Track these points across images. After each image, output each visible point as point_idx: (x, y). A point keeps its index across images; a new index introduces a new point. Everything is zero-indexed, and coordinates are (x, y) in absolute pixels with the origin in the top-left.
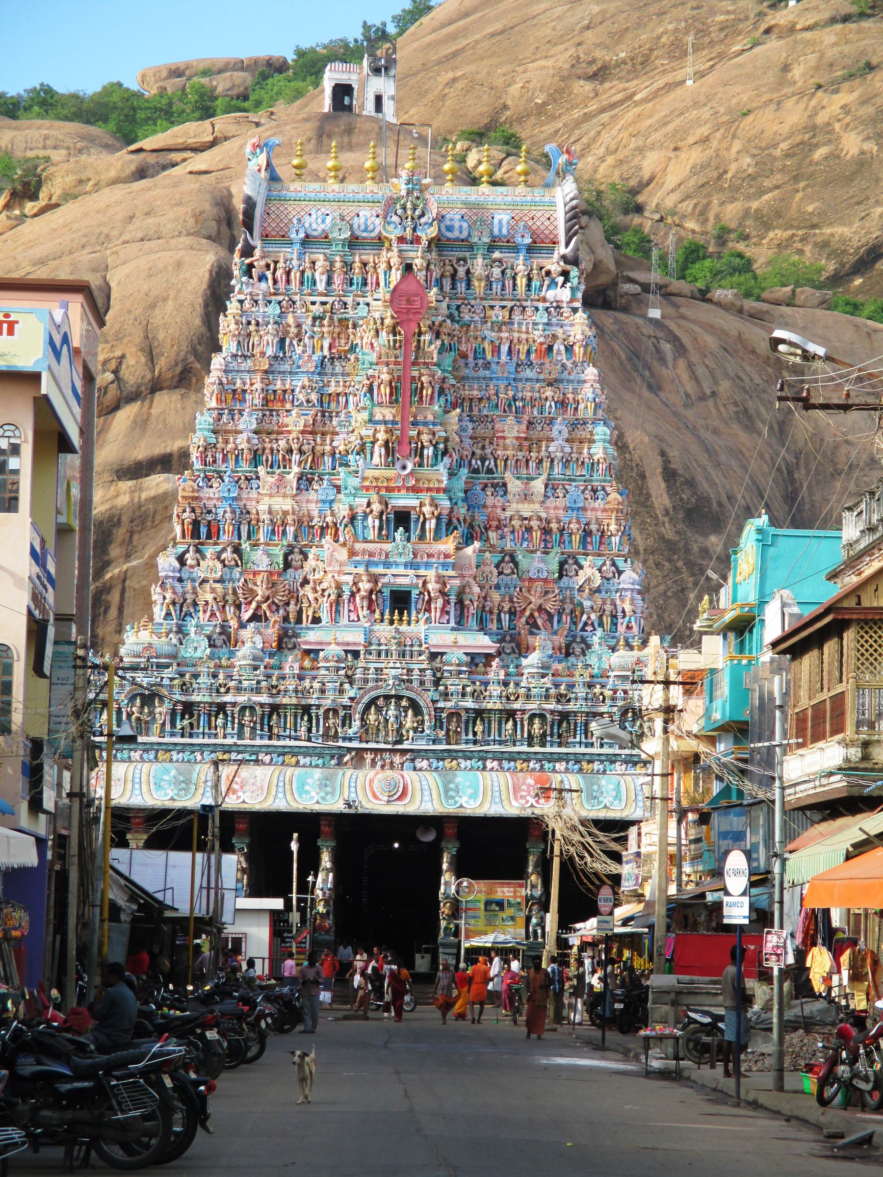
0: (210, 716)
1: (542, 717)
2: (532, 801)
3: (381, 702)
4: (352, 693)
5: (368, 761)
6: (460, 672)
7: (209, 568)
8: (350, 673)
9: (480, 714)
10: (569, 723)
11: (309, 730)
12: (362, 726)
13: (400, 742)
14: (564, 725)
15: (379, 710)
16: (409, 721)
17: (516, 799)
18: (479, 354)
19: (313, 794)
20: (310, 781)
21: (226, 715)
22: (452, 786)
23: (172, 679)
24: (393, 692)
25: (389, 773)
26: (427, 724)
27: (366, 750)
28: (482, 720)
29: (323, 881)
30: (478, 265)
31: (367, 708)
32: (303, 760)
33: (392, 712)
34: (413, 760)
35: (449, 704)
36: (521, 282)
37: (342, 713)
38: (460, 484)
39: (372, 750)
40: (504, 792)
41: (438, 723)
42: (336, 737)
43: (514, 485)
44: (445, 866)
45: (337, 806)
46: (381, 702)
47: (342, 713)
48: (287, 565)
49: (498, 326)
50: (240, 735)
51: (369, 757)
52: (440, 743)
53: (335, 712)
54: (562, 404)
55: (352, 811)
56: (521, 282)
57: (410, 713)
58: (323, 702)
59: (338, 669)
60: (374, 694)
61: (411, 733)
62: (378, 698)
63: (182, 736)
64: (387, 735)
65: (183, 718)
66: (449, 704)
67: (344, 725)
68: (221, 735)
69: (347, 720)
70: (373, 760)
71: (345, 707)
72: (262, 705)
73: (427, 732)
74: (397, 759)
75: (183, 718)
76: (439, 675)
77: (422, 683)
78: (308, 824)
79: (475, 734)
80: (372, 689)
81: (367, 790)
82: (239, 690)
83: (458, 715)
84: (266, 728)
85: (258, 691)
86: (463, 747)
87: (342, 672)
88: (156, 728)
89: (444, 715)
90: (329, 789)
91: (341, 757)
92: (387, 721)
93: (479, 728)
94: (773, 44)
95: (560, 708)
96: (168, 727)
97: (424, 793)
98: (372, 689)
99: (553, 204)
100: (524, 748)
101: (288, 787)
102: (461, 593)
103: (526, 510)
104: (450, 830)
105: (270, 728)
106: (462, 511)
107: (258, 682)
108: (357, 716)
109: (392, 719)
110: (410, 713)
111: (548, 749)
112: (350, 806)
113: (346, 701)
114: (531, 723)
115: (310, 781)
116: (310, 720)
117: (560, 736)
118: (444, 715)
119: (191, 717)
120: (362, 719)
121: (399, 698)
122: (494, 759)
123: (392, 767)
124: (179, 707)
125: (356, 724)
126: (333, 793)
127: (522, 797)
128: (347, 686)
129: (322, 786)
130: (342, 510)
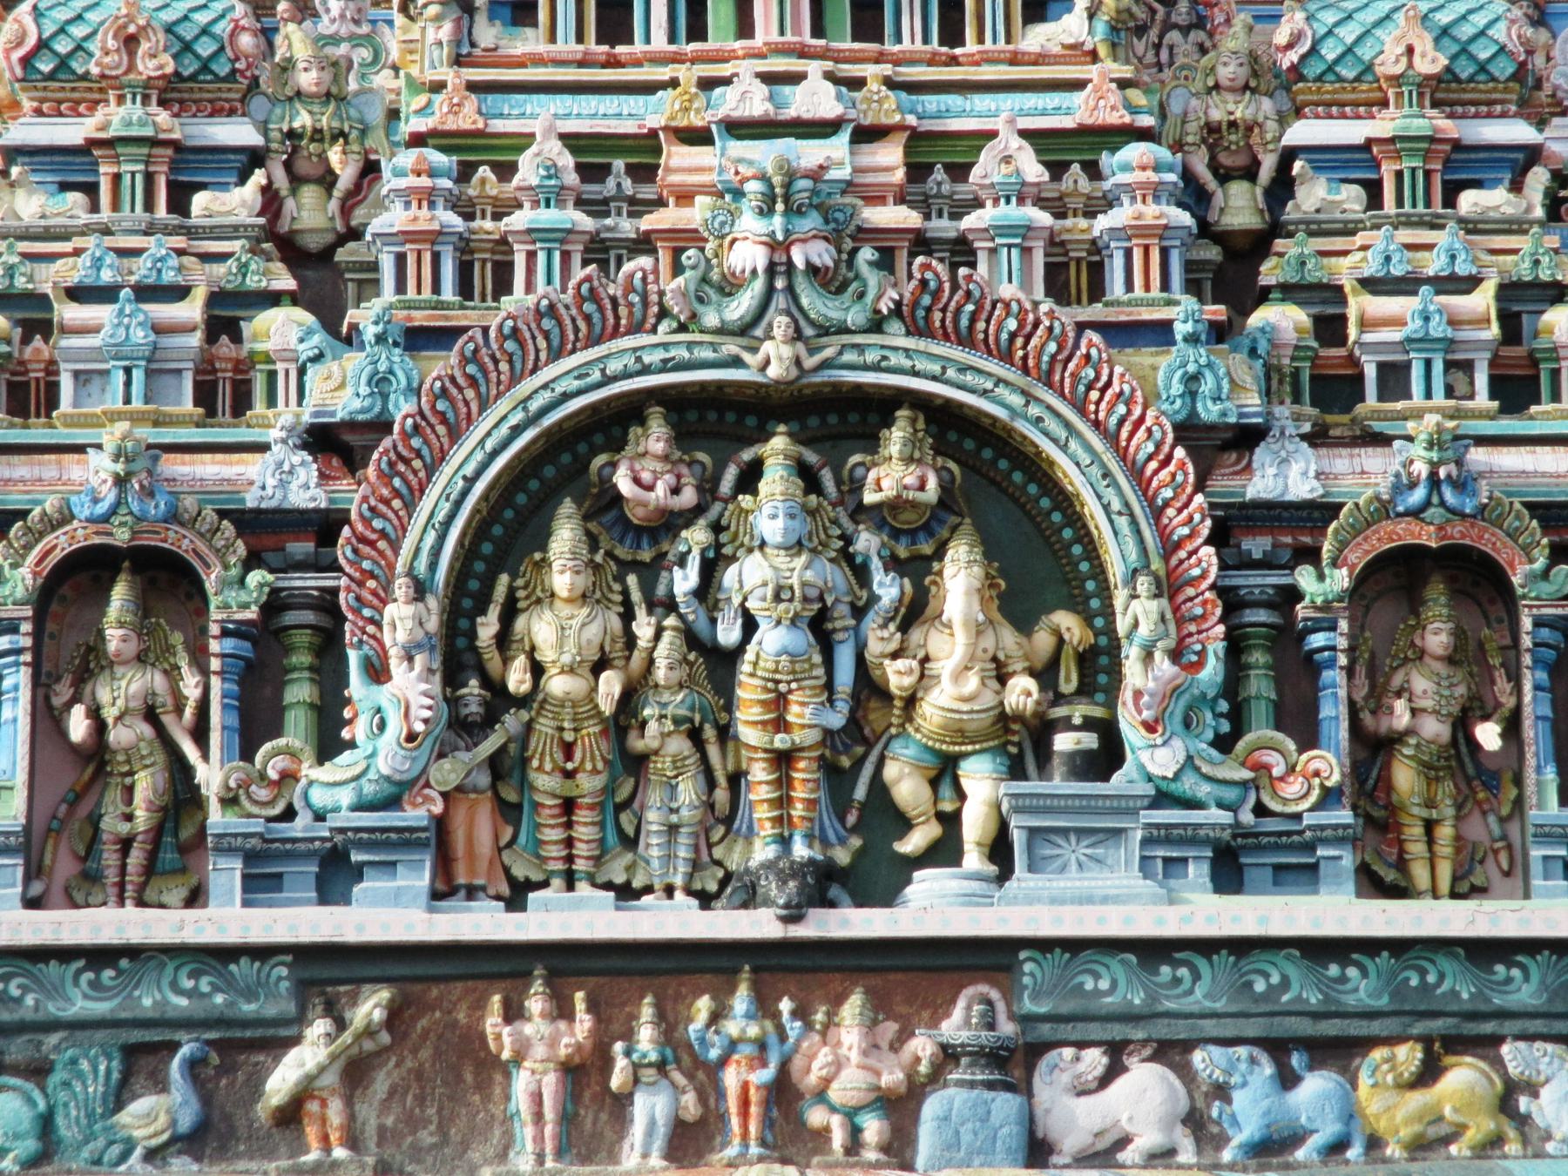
3: (645, 474)
4: (338, 390)
5: (532, 1086)
6: (1460, 167)
8: (310, 213)
12: (461, 728)
13: (878, 880)
15: (632, 550)
16: (954, 661)
24: (774, 360)
26: (1142, 676)
27: (506, 964)
31: (501, 540)
33: (767, 567)
34: (1011, 1064)
35: (1362, 475)
37: (234, 594)
39: (566, 963)
41: (1265, 670)
42: (176, 848)
46: (645, 474)
47: (234, 594)
51: (535, 1041)
52: (1302, 875)
53: (167, 580)
57: (960, 577)
59: (187, 171)
60: (565, 383)
61: (981, 782)
62: (612, 423)
64: (723, 816)
66: (1362, 475)
67: (256, 723)
69: (291, 665)
70: (583, 1074)
71: (263, 531)
73: (1152, 756)
74: (845, 1054)
76: (1239, 207)
77: (1073, 274)
80: (555, 332)
83: (1476, 578)
89: (1320, 585)
91: (244, 1046)
92: (718, 664)
98: (555, 332)
108: (402, 620)
109: (774, 640)
110: (960, 577)
118: (1320, 585)
120: (456, 658)
121: (838, 419)
125: (395, 702)
128: (280, 330)
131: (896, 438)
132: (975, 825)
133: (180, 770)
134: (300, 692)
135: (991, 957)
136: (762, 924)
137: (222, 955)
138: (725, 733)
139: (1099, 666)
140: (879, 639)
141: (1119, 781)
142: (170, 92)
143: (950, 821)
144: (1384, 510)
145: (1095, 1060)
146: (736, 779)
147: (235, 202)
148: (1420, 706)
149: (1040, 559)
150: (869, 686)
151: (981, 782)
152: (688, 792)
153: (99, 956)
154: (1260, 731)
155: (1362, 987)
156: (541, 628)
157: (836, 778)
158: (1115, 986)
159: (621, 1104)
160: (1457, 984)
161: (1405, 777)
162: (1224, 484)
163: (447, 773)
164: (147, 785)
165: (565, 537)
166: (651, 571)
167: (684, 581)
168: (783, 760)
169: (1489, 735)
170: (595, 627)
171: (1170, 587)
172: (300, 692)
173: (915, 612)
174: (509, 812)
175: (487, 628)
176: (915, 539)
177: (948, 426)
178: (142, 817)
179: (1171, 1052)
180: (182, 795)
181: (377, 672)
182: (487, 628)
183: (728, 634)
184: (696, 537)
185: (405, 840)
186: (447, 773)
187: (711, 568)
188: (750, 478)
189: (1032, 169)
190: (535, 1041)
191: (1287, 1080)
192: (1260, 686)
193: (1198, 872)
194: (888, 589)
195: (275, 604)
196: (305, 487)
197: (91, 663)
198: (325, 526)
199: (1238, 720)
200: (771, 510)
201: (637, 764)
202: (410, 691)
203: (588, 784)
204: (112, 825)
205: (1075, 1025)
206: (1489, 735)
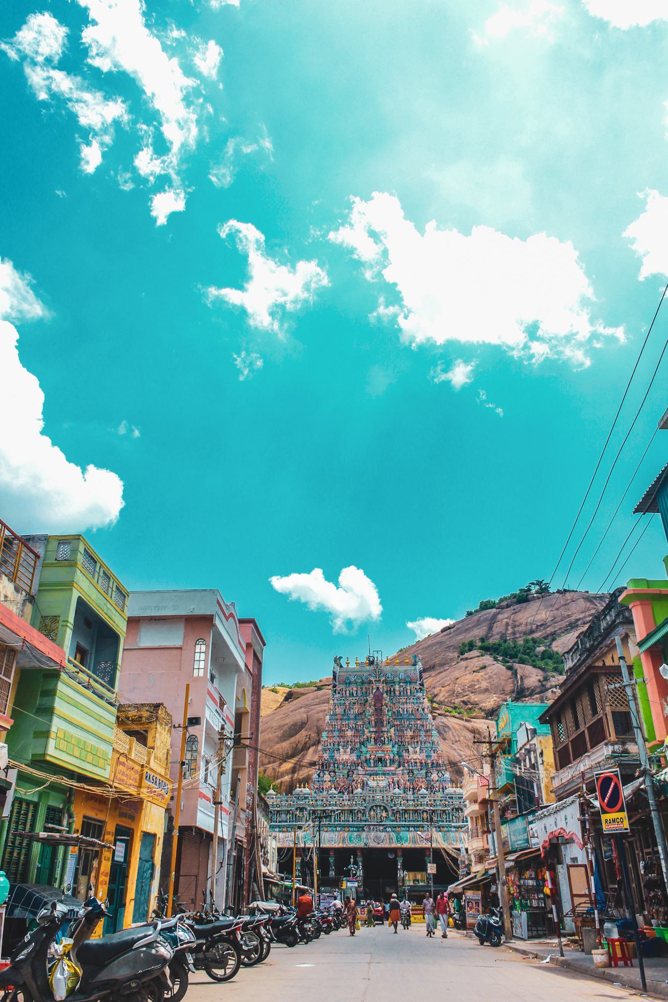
1: (426, 812)
7: (327, 777)
9: (406, 811)
16: (384, 814)
18: (398, 712)
30: (397, 688)
32: (351, 829)
36: (409, 692)
38: (395, 749)
41: (394, 814)
43: (411, 749)
45: (361, 845)
48: (348, 776)
49: (403, 704)
54: (423, 726)
56: (409, 692)
69: (364, 814)
74: (381, 828)
82: (330, 805)
85: (336, 805)
88: (304, 819)
94: (462, 662)
99: (415, 669)
102: (398, 782)
103: (415, 757)
104: (400, 853)
106: (397, 757)
121: (380, 806)
130: (363, 758)
149: (386, 811)
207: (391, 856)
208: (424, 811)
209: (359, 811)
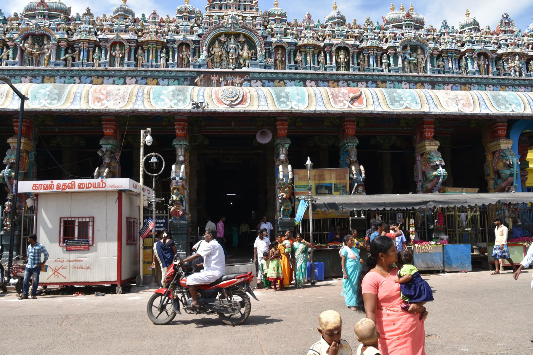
0: (88, 52)
1: (346, 49)
2: (348, 104)
3: (223, 39)
4: (200, 31)
5: (214, 82)
8: (199, 22)
9: (297, 49)
10: (364, 56)
11: (167, 60)
12: (209, 56)
14: (361, 56)
15: (222, 44)
16: (245, 53)
17: (335, 103)
19: (167, 101)
20: (165, 92)
21: (100, 50)
22: (282, 94)
23: (58, 25)
25: (230, 87)
26: (259, 54)
28: (300, 52)
29: (179, 172)
33: (232, 45)
39: (217, 73)
40: (325, 98)
41: (268, 54)
42: (188, 65)
44: (282, 157)
45: (187, 106)
47: (193, 46)
50: (112, 64)
51: (215, 78)
55: (200, 110)
57: (246, 47)
58: (177, 38)
62: (220, 35)
63: (66, 65)
65: (66, 52)
66: (274, 40)
68: (96, 65)
69: (196, 52)
70: (218, 81)
71: (195, 42)
72: (129, 41)
74: (238, 80)
75: (66, 52)
78: (162, 123)
79: (296, 62)
81: (214, 99)
84: (132, 57)
85: (126, 31)
86: (288, 71)
87: (193, 20)
90: (181, 98)
92: (228, 53)
93: (299, 58)
95: (358, 43)
96: (53, 58)
97: (260, 99)
100: (334, 71)
101: (146, 96)
105: (136, 59)
107: (127, 26)
108: (204, 48)
110: (246, 47)
111: (351, 72)
112: (198, 107)
113: (194, 38)
114: (338, 56)
115: (165, 92)
116: (167, 53)
117: (358, 64)
119: (74, 51)
120: (209, 52)
121: (237, 35)
122: (311, 80)
123: (233, 84)
124: (63, 44)
125: (204, 54)
126: (184, 100)
127: (340, 101)
129: (175, 95)
131: (241, 36)
132: (247, 64)
133: (188, 59)
134: (197, 54)
135: (247, 73)
136: (231, 70)
137: (191, 72)
138: (228, 58)
139: (256, 54)
140: (240, 51)
141: (258, 61)
142: (189, 12)
143: (245, 64)
144: (276, 42)
145: (255, 81)
146: (229, 61)
147: (193, 20)
148: (279, 57)
150: (239, 55)
151: (247, 62)
152: (226, 62)
153: (182, 71)
154: (267, 58)
155: (274, 76)
156: (214, 49)
157: (237, 61)
158: (256, 75)
159: (221, 83)
160: (281, 76)
161: (277, 62)
162: (265, 40)
163: (208, 59)
164: (186, 60)
165: (217, 42)
166: (223, 46)
167: (225, 46)
168: (233, 59)
169: (283, 59)
170: (219, 50)
171: (261, 47)
172: (197, 54)
173: (242, 49)
174: (212, 63)
175: (211, 49)
176: (243, 45)
177: (245, 36)
178: (186, 63)
179: (261, 81)
180: (189, 61)
181: (203, 52)
182: (211, 49)
183: (229, 50)
184: (226, 43)
185: (205, 64)
186: (208, 59)
187: (227, 46)
188: (230, 39)
189: (251, 19)
190: (215, 78)
191: (269, 82)
192: (267, 55)
193: (263, 67)
194: (240, 47)
195: (195, 47)
196: (197, 39)
197: (182, 51)
198: (199, 41)
199: (266, 57)
200: (232, 41)
201: (222, 60)
202: (205, 53)
203: (218, 61)
204: (183, 63)
205: (253, 78)
206: (283, 59)
207: (264, 140)
208: (339, 49)
209: (185, 44)
